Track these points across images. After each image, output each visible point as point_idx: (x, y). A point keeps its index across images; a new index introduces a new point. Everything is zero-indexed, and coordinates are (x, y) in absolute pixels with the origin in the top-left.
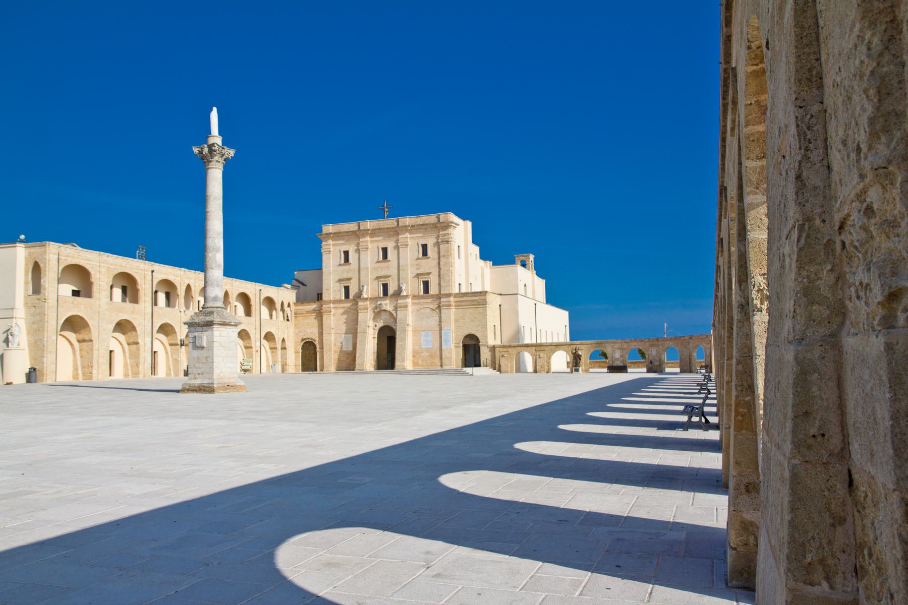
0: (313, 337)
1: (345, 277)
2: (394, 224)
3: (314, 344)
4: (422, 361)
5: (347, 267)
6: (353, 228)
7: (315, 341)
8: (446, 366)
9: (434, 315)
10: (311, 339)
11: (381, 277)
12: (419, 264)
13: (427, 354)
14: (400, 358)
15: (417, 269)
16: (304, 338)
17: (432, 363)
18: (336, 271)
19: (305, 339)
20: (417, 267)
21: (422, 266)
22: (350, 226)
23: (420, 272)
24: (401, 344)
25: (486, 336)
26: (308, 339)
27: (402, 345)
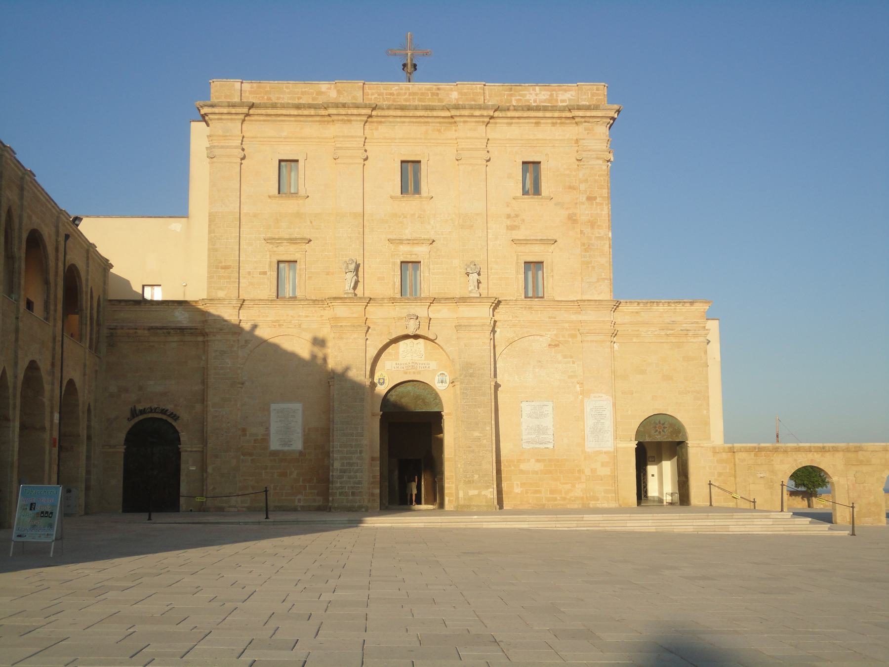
0: (170, 407)
1: (287, 236)
2: (440, 100)
3: (173, 427)
4: (522, 484)
5: (289, 206)
6: (314, 99)
7: (176, 417)
8: (598, 500)
9: (560, 357)
10: (164, 412)
11: (401, 241)
12: (517, 216)
13: (539, 466)
14: (476, 477)
15: (511, 228)
16: (140, 407)
17: (552, 492)
18: (255, 215)
19: (143, 412)
20: (509, 222)
21: (523, 220)
22: (303, 93)
23: (519, 235)
24: (476, 434)
25: (706, 423)
26: (152, 410)
27: (479, 439)
